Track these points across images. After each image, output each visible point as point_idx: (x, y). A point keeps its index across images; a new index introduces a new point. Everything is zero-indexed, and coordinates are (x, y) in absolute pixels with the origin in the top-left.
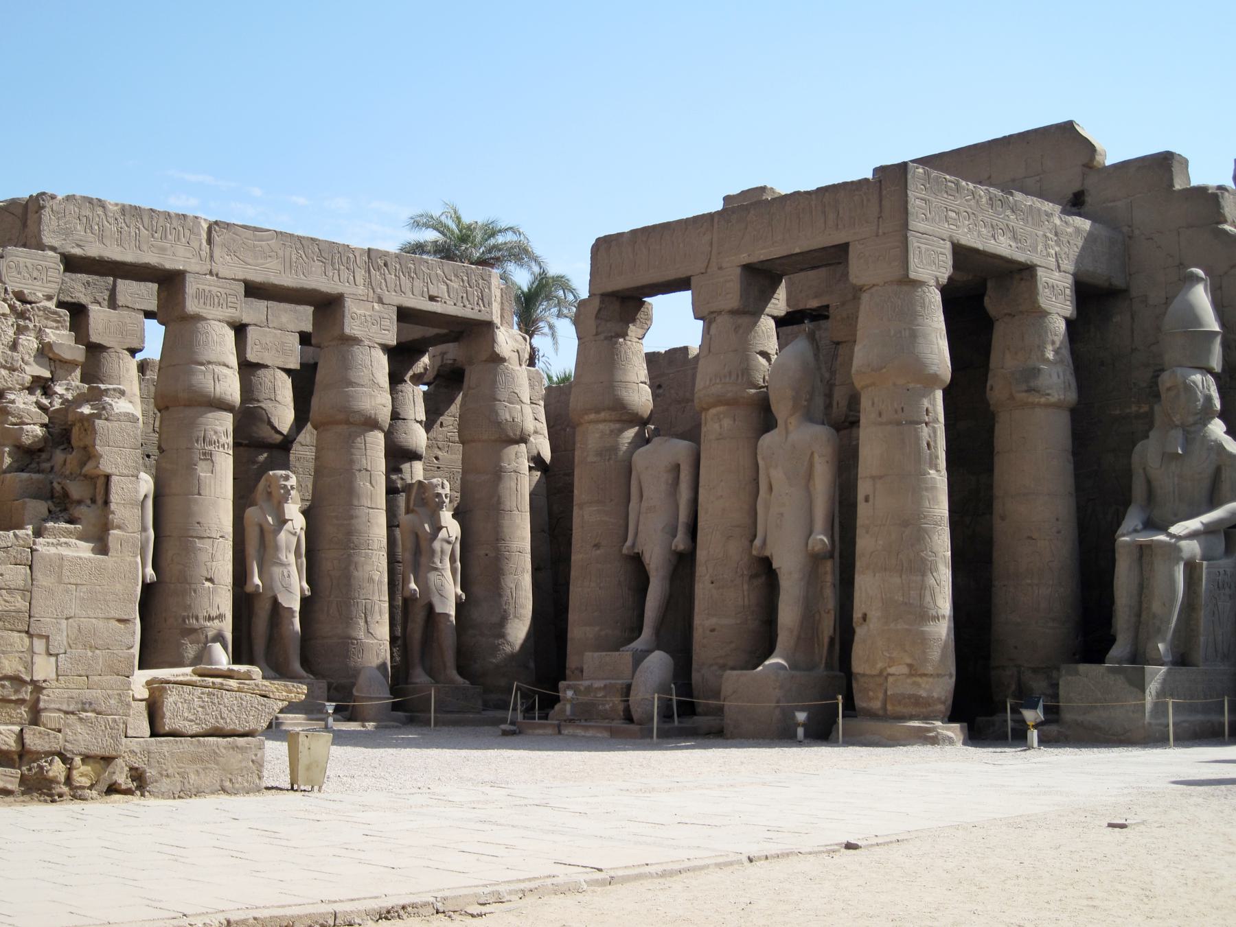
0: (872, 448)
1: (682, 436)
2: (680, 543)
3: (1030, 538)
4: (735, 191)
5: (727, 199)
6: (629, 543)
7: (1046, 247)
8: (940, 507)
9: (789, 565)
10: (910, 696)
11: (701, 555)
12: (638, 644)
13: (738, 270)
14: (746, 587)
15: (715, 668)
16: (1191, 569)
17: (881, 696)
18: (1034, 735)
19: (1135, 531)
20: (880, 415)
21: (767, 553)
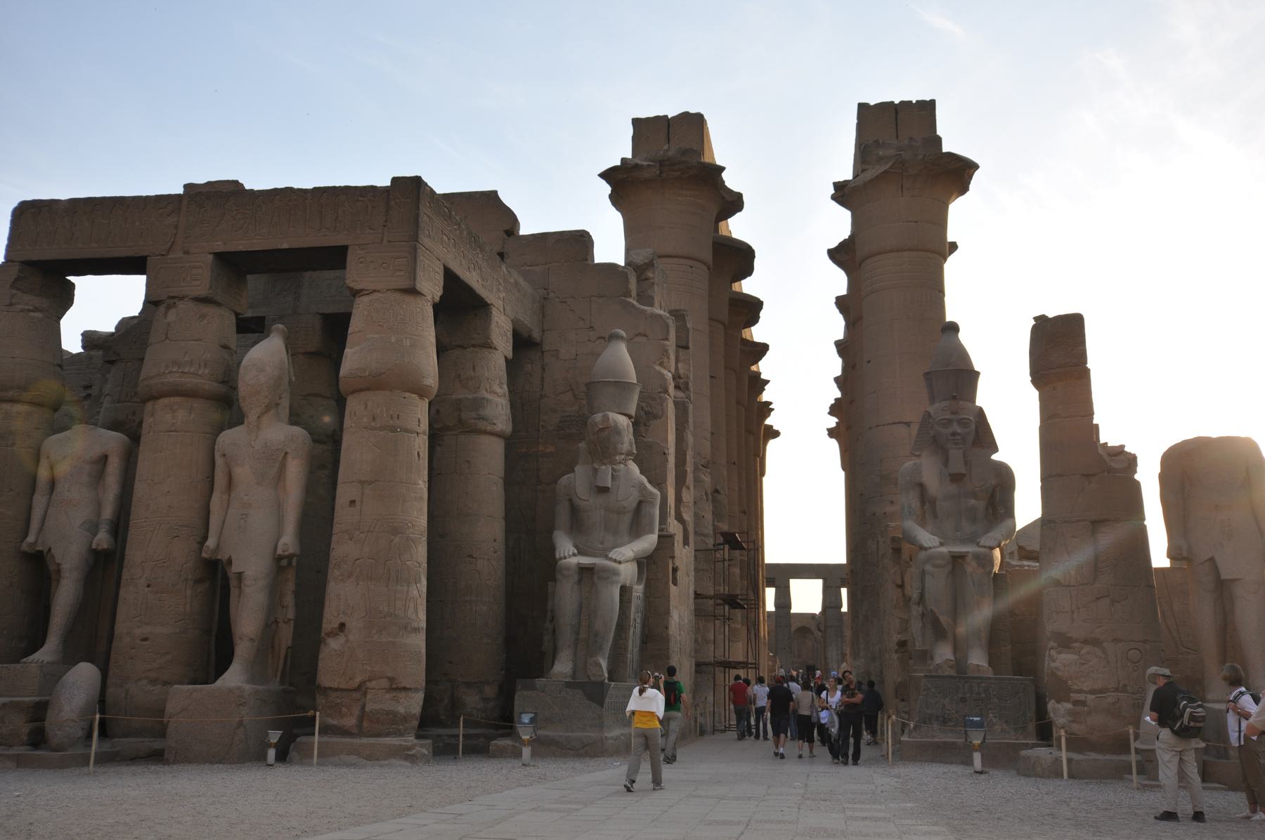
0: (357, 453)
1: (114, 426)
2: (103, 539)
3: (471, 556)
4: (201, 180)
5: (187, 187)
6: (31, 538)
7: (498, 290)
8: (419, 518)
9: (252, 566)
10: (388, 713)
11: (135, 554)
12: (47, 653)
13: (211, 257)
14: (189, 592)
15: (144, 682)
16: (625, 591)
17: (356, 712)
18: (526, 751)
19: (574, 555)
20: (374, 419)
21: (223, 556)
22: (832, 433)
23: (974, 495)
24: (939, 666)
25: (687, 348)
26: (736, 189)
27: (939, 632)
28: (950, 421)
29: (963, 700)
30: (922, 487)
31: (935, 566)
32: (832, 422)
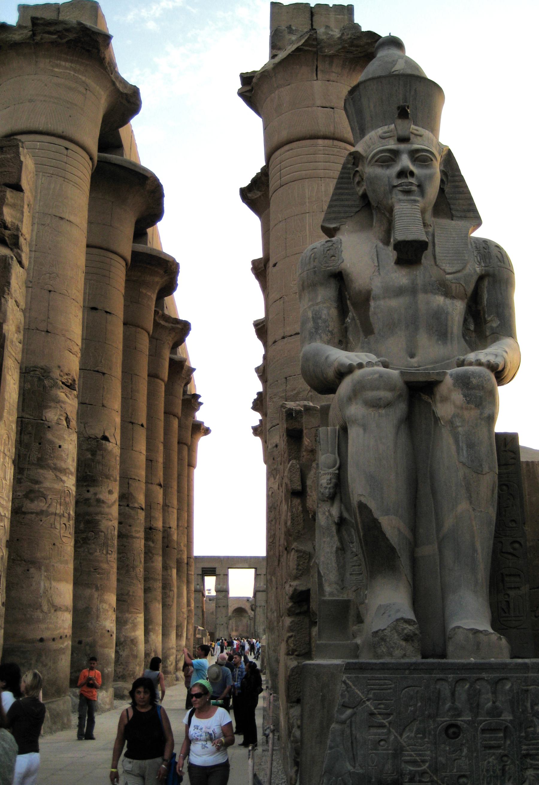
22: (257, 431)
23: (444, 288)
24: (379, 637)
25: (18, 188)
26: (132, 81)
27: (376, 554)
28: (395, 154)
29: (452, 731)
30: (339, 278)
31: (375, 405)
32: (256, 418)
